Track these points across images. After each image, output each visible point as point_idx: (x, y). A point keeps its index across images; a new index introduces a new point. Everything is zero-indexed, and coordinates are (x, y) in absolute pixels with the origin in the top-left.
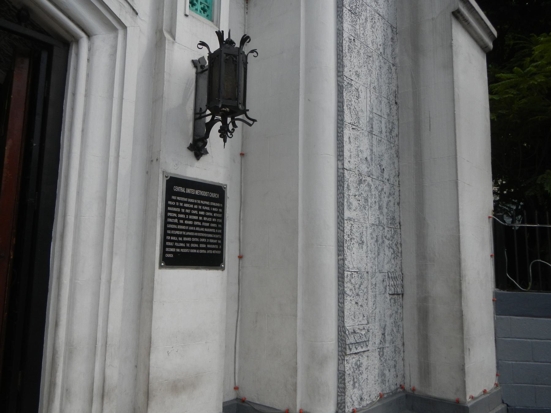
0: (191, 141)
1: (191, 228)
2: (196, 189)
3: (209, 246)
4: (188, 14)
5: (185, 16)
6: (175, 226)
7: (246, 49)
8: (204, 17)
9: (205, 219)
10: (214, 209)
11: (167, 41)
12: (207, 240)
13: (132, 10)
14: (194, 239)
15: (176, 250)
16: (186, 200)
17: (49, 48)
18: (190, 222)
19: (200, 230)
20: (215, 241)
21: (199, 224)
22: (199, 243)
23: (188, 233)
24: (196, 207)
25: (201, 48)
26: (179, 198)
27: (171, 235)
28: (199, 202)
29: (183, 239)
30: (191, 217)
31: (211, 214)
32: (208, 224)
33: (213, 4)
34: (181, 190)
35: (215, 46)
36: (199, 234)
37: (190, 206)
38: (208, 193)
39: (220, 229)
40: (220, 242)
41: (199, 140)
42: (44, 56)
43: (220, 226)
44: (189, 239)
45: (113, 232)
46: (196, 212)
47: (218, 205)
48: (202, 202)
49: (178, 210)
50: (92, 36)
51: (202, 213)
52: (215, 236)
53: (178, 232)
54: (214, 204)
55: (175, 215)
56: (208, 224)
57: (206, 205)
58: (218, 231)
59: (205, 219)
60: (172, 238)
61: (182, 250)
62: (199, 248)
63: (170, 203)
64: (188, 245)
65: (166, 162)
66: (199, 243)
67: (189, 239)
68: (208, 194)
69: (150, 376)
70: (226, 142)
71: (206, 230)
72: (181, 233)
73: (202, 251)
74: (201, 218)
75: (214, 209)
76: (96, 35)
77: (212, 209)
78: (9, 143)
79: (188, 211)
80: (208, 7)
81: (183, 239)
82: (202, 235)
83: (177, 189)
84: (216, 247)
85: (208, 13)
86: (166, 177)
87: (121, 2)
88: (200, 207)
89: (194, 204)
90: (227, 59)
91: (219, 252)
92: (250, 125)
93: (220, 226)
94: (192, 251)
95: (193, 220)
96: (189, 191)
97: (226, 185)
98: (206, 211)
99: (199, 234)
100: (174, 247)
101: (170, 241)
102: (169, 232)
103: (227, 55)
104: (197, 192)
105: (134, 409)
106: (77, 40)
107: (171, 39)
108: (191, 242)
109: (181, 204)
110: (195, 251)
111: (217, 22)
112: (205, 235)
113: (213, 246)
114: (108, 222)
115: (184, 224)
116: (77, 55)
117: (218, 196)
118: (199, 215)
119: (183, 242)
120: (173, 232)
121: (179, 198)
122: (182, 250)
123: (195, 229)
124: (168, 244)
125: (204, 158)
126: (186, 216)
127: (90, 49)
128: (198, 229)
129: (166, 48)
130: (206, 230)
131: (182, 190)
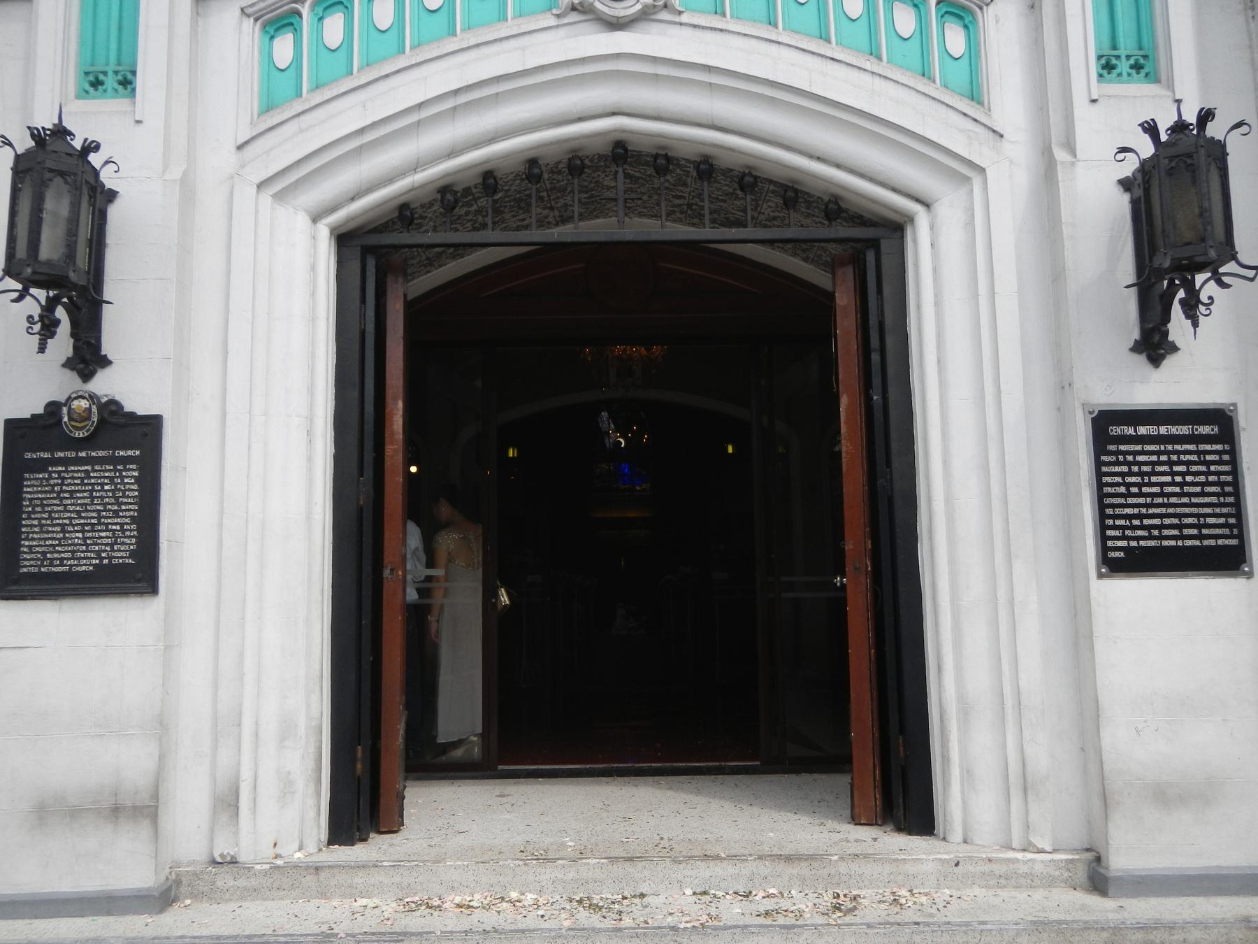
0: (1136, 335)
1: (1160, 500)
2: (1159, 424)
3: (1205, 531)
4: (1096, 98)
5: (1094, 103)
6: (1122, 501)
7: (1214, 130)
8: (1139, 81)
9: (1189, 479)
10: (1208, 458)
11: (1059, 167)
12: (1199, 521)
13: (991, 133)
14: (1167, 521)
15: (1129, 544)
16: (1139, 448)
17: (874, 244)
18: (1156, 490)
19: (1179, 502)
20: (1222, 521)
21: (1177, 490)
22: (1180, 527)
23: (1151, 511)
24: (1164, 458)
25: (1123, 158)
26: (1122, 448)
27: (1115, 517)
28: (1170, 447)
29: (1142, 522)
30: (1154, 479)
31: (1203, 468)
32: (1198, 489)
33: (1155, 48)
34: (1126, 431)
35: (1146, 148)
36: (1179, 510)
37: (1149, 458)
38: (1190, 427)
39: (1231, 496)
40: (1232, 521)
41: (1153, 330)
42: (870, 257)
43: (1228, 489)
44: (1156, 521)
45: (1007, 521)
46: (1166, 468)
48: (1178, 447)
49: (1125, 469)
50: (932, 205)
51: (1182, 468)
52: (1218, 510)
53: (1129, 511)
54: (1208, 447)
55: (1118, 479)
56: (1198, 489)
58: (1225, 499)
59: (1189, 479)
60: (1118, 522)
61: (1143, 543)
62: (1183, 537)
63: (1104, 458)
64: (1155, 533)
65: (1086, 386)
66: (1180, 527)
67: (1156, 521)
68: (1189, 429)
69: (1105, 767)
70: (1198, 327)
71: (1194, 500)
72: (1136, 511)
73: (1189, 543)
74: (1178, 479)
75: (1208, 458)
76: (937, 201)
77: (1205, 457)
78: (844, 401)
79: (1145, 468)
80: (1145, 57)
81: (1142, 522)
82: (1187, 510)
83: (1116, 430)
84: (1226, 531)
85: (1146, 70)
86: (1091, 413)
87: (971, 129)
88: (1174, 458)
89: (1158, 453)
90: (1172, 168)
91: (1234, 542)
92: (1252, 280)
93: (1228, 489)
94: (1165, 543)
95: (1162, 485)
96: (1143, 430)
97: (1234, 405)
98: (1188, 463)
99: (1179, 510)
101: (1115, 527)
102: (1109, 511)
103: (1171, 158)
104: (1163, 430)
105: (1089, 822)
106: (911, 219)
107: (1069, 158)
108: (1160, 527)
109: (1130, 458)
110: (1173, 543)
111: (1168, 80)
112: (1194, 510)
113: (1217, 531)
114: (996, 504)
115: (1141, 495)
116: (915, 241)
117: (1216, 429)
118: (1173, 474)
119: (1142, 527)
120: (1118, 511)
121: (1122, 448)
122: (1143, 543)
123: (1168, 500)
125: (1170, 362)
126: (1143, 479)
127: (932, 227)
128: (1173, 500)
129: (1060, 179)
130: (1194, 500)
131: (1130, 431)
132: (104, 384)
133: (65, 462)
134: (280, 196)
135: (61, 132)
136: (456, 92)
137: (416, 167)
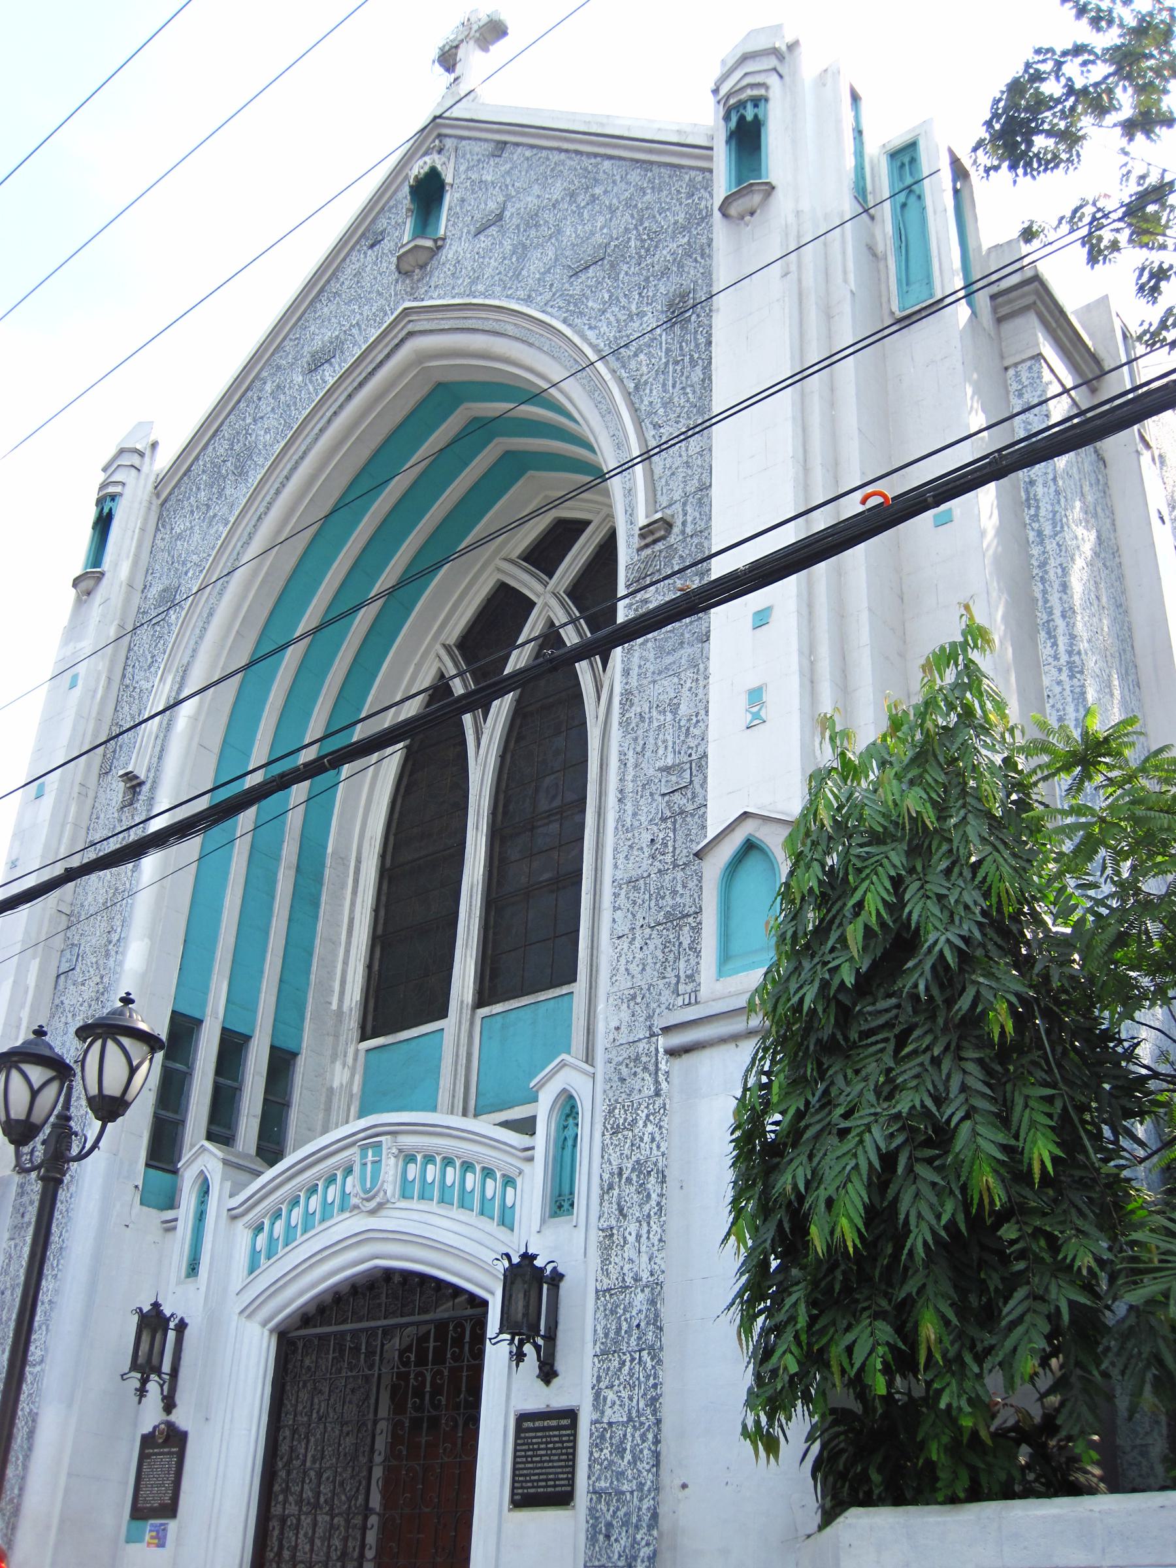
16: (533, 1434)
22: (546, 1480)
44: (536, 1477)
47: (569, 1432)
51: (550, 1446)
57: (555, 1436)
67: (536, 1477)
73: (549, 1490)
83: (526, 1425)
84: (566, 1482)
89: (542, 1437)
91: (569, 1489)
95: (541, 1456)
96: (537, 1424)
100: (522, 1488)
101: (519, 1482)
104: (546, 1424)
108: (537, 1481)
115: (532, 1462)
118: (547, 1449)
124: (516, 1485)
125: (556, 1382)
131: (530, 1424)
132: (173, 1418)
133: (156, 1454)
134: (249, 1317)
135: (156, 1305)
136: (310, 1257)
137: (301, 1294)
